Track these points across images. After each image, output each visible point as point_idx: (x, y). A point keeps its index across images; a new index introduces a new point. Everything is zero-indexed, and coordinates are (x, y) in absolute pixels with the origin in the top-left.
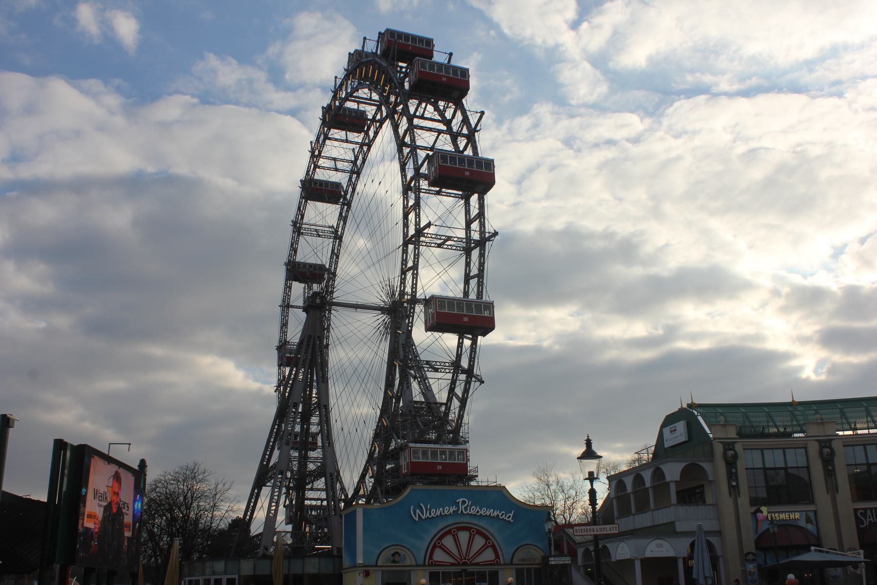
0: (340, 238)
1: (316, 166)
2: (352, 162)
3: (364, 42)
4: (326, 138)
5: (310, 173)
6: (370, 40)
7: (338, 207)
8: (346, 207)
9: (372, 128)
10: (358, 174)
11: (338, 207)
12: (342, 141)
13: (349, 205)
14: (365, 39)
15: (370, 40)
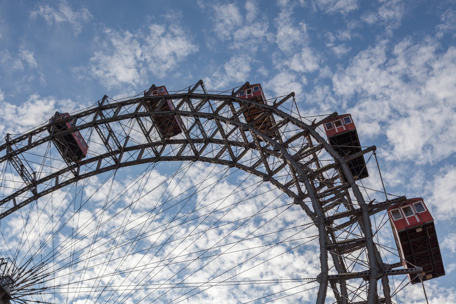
0: (37, 196)
1: (94, 124)
2: (120, 147)
3: (288, 97)
4: (136, 115)
5: (79, 123)
6: (294, 99)
7: (64, 165)
8: (71, 176)
9: (177, 147)
10: (118, 165)
11: (64, 165)
12: (144, 130)
13: (77, 177)
14: (293, 94)
15: (294, 99)
